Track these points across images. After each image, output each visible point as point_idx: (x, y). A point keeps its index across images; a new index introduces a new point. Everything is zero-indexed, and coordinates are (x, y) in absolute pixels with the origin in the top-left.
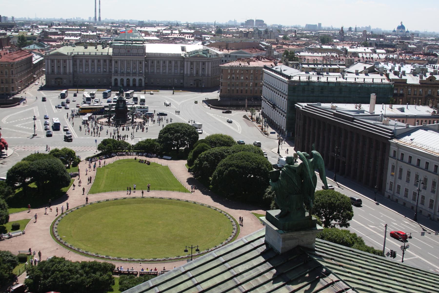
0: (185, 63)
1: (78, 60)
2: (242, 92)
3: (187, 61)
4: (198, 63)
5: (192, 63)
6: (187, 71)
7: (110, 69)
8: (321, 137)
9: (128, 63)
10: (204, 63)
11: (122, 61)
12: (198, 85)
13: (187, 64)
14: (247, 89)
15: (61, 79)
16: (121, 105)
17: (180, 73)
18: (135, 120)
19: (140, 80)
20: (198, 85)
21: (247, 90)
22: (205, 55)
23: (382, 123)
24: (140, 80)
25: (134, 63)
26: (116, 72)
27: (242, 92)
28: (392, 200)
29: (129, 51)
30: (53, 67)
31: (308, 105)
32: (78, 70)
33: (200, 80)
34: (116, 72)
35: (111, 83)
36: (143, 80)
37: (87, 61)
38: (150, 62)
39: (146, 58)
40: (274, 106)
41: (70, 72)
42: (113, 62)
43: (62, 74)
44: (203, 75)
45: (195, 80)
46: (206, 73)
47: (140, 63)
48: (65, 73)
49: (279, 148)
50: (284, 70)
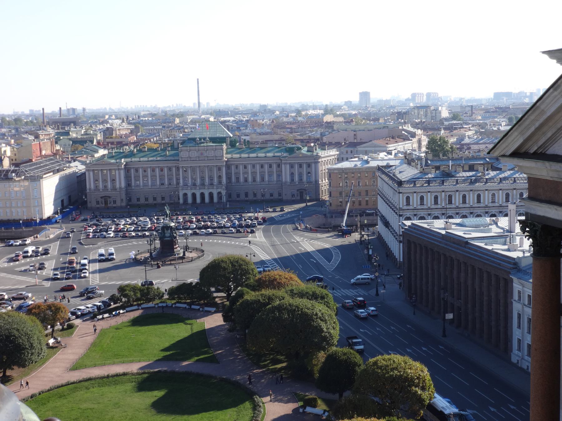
0: (283, 166)
1: (132, 170)
2: (360, 205)
3: (285, 163)
4: (300, 166)
5: (292, 166)
6: (286, 177)
7: (178, 179)
8: (430, 272)
9: (202, 172)
10: (309, 166)
11: (193, 169)
12: (302, 196)
13: (286, 169)
14: (367, 199)
15: (110, 197)
16: (168, 233)
17: (277, 181)
18: (187, 254)
19: (219, 193)
20: (302, 196)
21: (367, 201)
22: (309, 153)
23: (506, 247)
24: (219, 193)
25: (210, 169)
26: (185, 185)
27: (360, 205)
28: (521, 369)
29: (202, 154)
30: (97, 181)
31: (412, 224)
32: (133, 184)
33: (305, 190)
34: (185, 185)
35: (179, 199)
36: (224, 193)
37: (145, 171)
38: (233, 168)
39: (226, 162)
40: (387, 224)
41: (120, 188)
42: (181, 170)
43: (110, 190)
44: (309, 182)
45: (298, 190)
46: (314, 179)
47: (219, 169)
48: (114, 189)
49: (377, 289)
50: (400, 172)
